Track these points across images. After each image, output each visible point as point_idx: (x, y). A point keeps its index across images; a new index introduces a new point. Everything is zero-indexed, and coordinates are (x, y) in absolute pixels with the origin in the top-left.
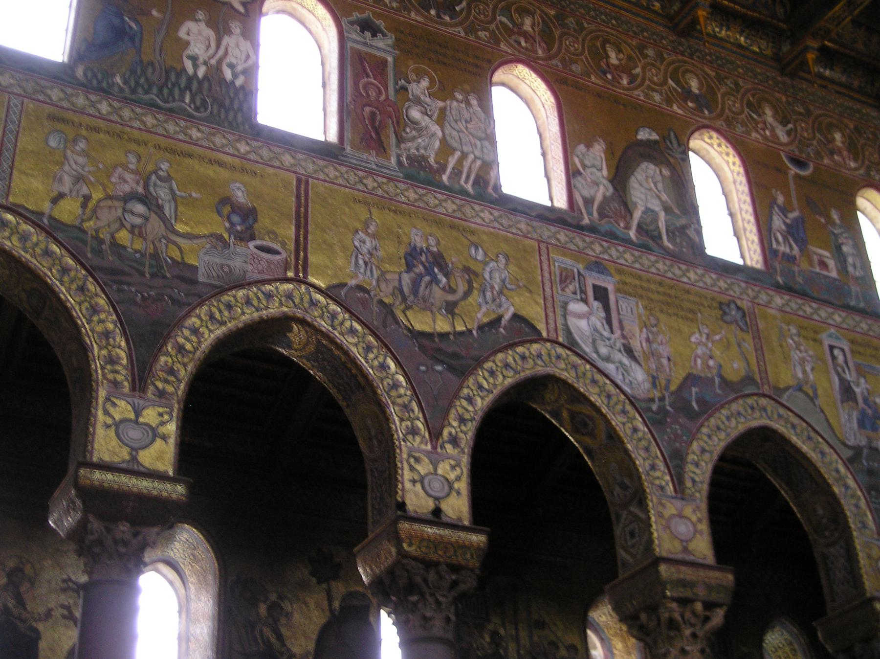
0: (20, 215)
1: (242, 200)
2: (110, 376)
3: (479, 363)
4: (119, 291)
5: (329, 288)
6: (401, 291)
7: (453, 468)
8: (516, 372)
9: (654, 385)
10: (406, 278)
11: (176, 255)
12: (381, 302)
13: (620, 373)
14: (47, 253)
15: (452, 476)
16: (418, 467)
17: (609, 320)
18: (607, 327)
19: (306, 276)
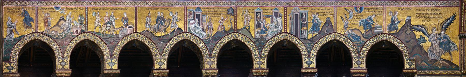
0: (90, 33)
1: (126, 17)
2: (107, 56)
3: (170, 40)
4: (107, 42)
5: (141, 33)
6: (155, 29)
7: (164, 60)
8: (178, 40)
9: (208, 36)
10: (156, 25)
11: (115, 33)
12: (151, 33)
13: (200, 35)
14: (95, 38)
15: (163, 62)
16: (157, 61)
17: (199, 23)
18: (198, 25)
19: (137, 31)
